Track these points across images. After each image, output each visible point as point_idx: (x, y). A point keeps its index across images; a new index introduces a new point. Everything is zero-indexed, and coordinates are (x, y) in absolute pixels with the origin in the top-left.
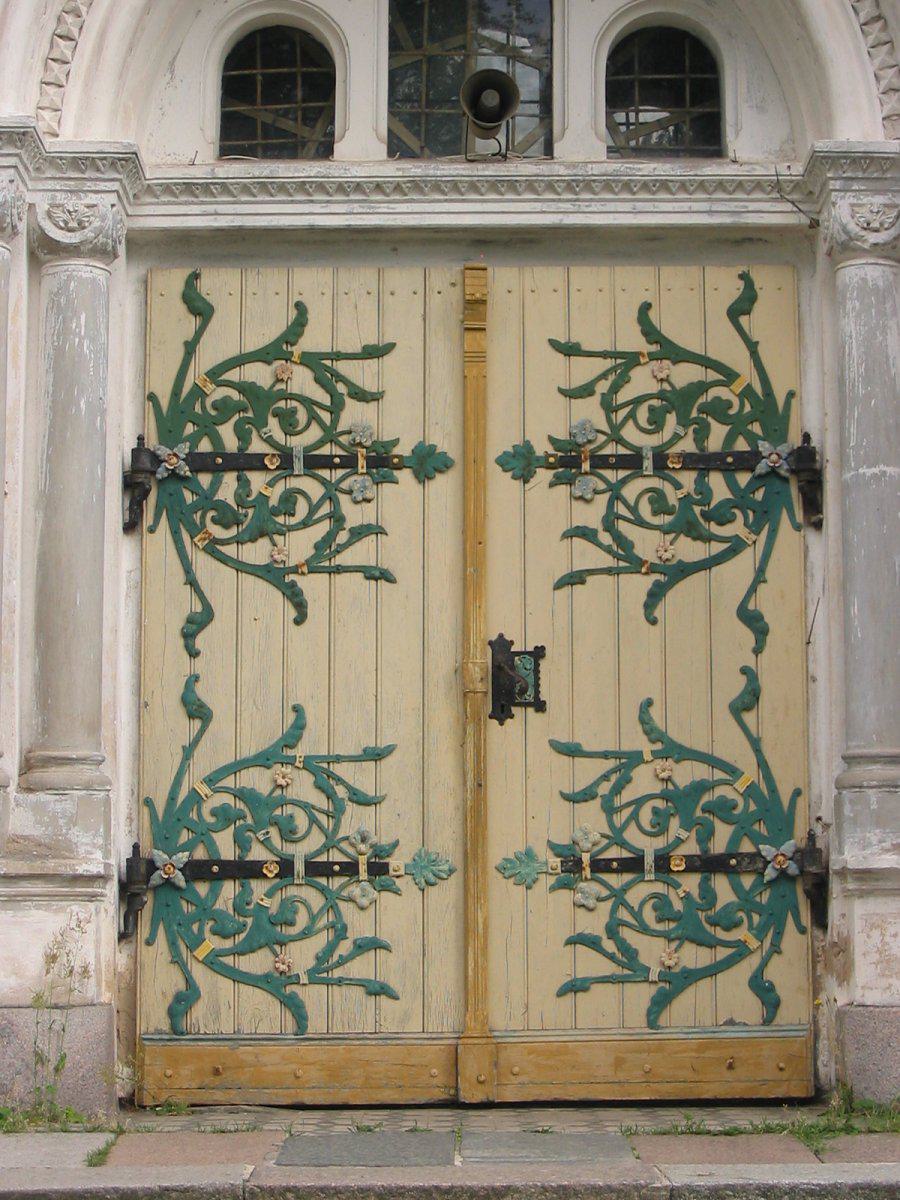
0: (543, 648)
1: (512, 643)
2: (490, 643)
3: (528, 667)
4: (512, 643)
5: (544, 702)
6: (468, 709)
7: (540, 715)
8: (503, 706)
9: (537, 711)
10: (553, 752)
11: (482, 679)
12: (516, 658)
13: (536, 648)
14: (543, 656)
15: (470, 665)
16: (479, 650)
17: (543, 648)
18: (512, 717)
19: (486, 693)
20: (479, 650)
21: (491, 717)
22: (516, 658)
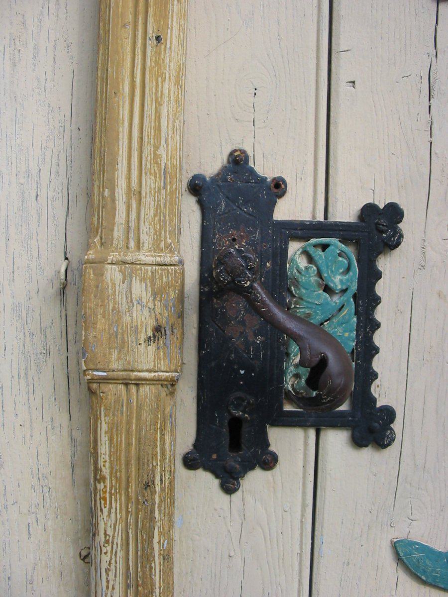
0: (394, 213)
1: (278, 187)
2: (196, 187)
3: (337, 281)
4: (278, 187)
5: (389, 414)
6: (104, 448)
7: (367, 454)
8: (235, 425)
9: (358, 442)
10: (403, 577)
11: (158, 329)
12: (294, 247)
13: (369, 210)
14: (392, 243)
15: (113, 274)
16: (149, 211)
17: (394, 213)
18: (269, 462)
19: (172, 384)
20: (149, 211)
21: (190, 463)
22: (294, 247)
